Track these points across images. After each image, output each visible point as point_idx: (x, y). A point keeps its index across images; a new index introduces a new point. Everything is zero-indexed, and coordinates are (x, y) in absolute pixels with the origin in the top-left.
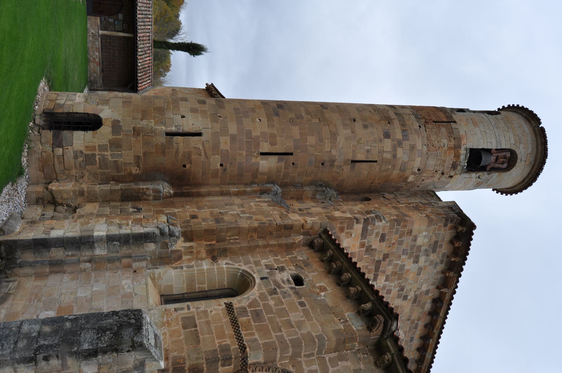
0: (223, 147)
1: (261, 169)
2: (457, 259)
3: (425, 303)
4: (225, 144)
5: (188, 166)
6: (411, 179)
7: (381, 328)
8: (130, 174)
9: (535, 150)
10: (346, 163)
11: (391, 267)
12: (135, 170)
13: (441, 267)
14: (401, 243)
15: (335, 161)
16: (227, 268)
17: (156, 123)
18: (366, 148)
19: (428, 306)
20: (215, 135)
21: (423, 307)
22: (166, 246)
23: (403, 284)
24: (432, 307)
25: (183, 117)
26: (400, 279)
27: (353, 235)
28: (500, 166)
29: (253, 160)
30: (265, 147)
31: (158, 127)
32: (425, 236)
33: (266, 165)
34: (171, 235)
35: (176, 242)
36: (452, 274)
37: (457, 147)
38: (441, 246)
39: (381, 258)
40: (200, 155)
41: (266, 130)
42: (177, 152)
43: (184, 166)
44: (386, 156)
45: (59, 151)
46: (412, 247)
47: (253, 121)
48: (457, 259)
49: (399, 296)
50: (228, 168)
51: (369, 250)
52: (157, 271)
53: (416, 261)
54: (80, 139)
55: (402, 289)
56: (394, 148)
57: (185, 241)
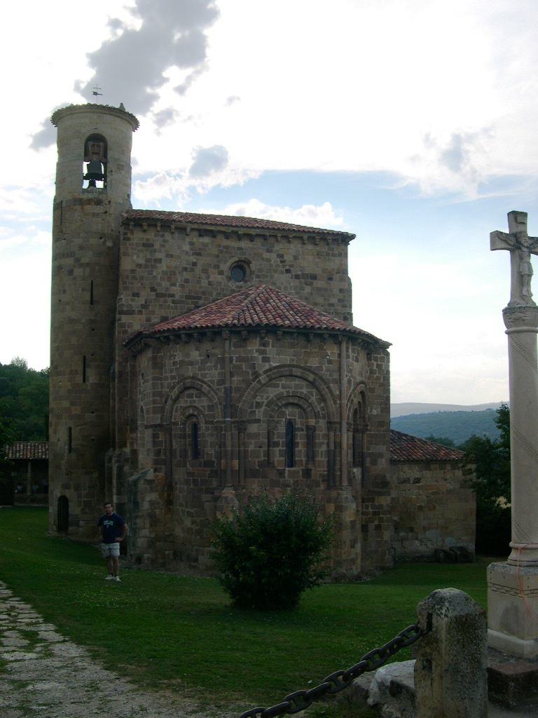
1: (97, 382)
2: (159, 224)
3: (203, 244)
4: (76, 410)
5: (93, 438)
6: (109, 244)
7: (149, 339)
12: (96, 475)
13: (168, 236)
14: (142, 278)
15: (91, 320)
18: (80, 292)
19: (206, 240)
21: (206, 245)
22: (126, 460)
23: (180, 269)
24: (207, 235)
25: (59, 440)
26: (175, 272)
27: (131, 321)
28: (102, 149)
29: (89, 388)
30: (79, 379)
31: (66, 458)
32: (138, 257)
33: (92, 378)
35: (125, 453)
36: (173, 227)
37: (81, 202)
38: (148, 239)
39: (154, 293)
43: (93, 440)
44: (87, 274)
45: (82, 523)
46: (146, 266)
48: (159, 224)
49: (192, 270)
51: (145, 306)
52: (140, 467)
53: (160, 261)
54: (74, 509)
55: (185, 269)
56: (81, 265)
57: (126, 447)
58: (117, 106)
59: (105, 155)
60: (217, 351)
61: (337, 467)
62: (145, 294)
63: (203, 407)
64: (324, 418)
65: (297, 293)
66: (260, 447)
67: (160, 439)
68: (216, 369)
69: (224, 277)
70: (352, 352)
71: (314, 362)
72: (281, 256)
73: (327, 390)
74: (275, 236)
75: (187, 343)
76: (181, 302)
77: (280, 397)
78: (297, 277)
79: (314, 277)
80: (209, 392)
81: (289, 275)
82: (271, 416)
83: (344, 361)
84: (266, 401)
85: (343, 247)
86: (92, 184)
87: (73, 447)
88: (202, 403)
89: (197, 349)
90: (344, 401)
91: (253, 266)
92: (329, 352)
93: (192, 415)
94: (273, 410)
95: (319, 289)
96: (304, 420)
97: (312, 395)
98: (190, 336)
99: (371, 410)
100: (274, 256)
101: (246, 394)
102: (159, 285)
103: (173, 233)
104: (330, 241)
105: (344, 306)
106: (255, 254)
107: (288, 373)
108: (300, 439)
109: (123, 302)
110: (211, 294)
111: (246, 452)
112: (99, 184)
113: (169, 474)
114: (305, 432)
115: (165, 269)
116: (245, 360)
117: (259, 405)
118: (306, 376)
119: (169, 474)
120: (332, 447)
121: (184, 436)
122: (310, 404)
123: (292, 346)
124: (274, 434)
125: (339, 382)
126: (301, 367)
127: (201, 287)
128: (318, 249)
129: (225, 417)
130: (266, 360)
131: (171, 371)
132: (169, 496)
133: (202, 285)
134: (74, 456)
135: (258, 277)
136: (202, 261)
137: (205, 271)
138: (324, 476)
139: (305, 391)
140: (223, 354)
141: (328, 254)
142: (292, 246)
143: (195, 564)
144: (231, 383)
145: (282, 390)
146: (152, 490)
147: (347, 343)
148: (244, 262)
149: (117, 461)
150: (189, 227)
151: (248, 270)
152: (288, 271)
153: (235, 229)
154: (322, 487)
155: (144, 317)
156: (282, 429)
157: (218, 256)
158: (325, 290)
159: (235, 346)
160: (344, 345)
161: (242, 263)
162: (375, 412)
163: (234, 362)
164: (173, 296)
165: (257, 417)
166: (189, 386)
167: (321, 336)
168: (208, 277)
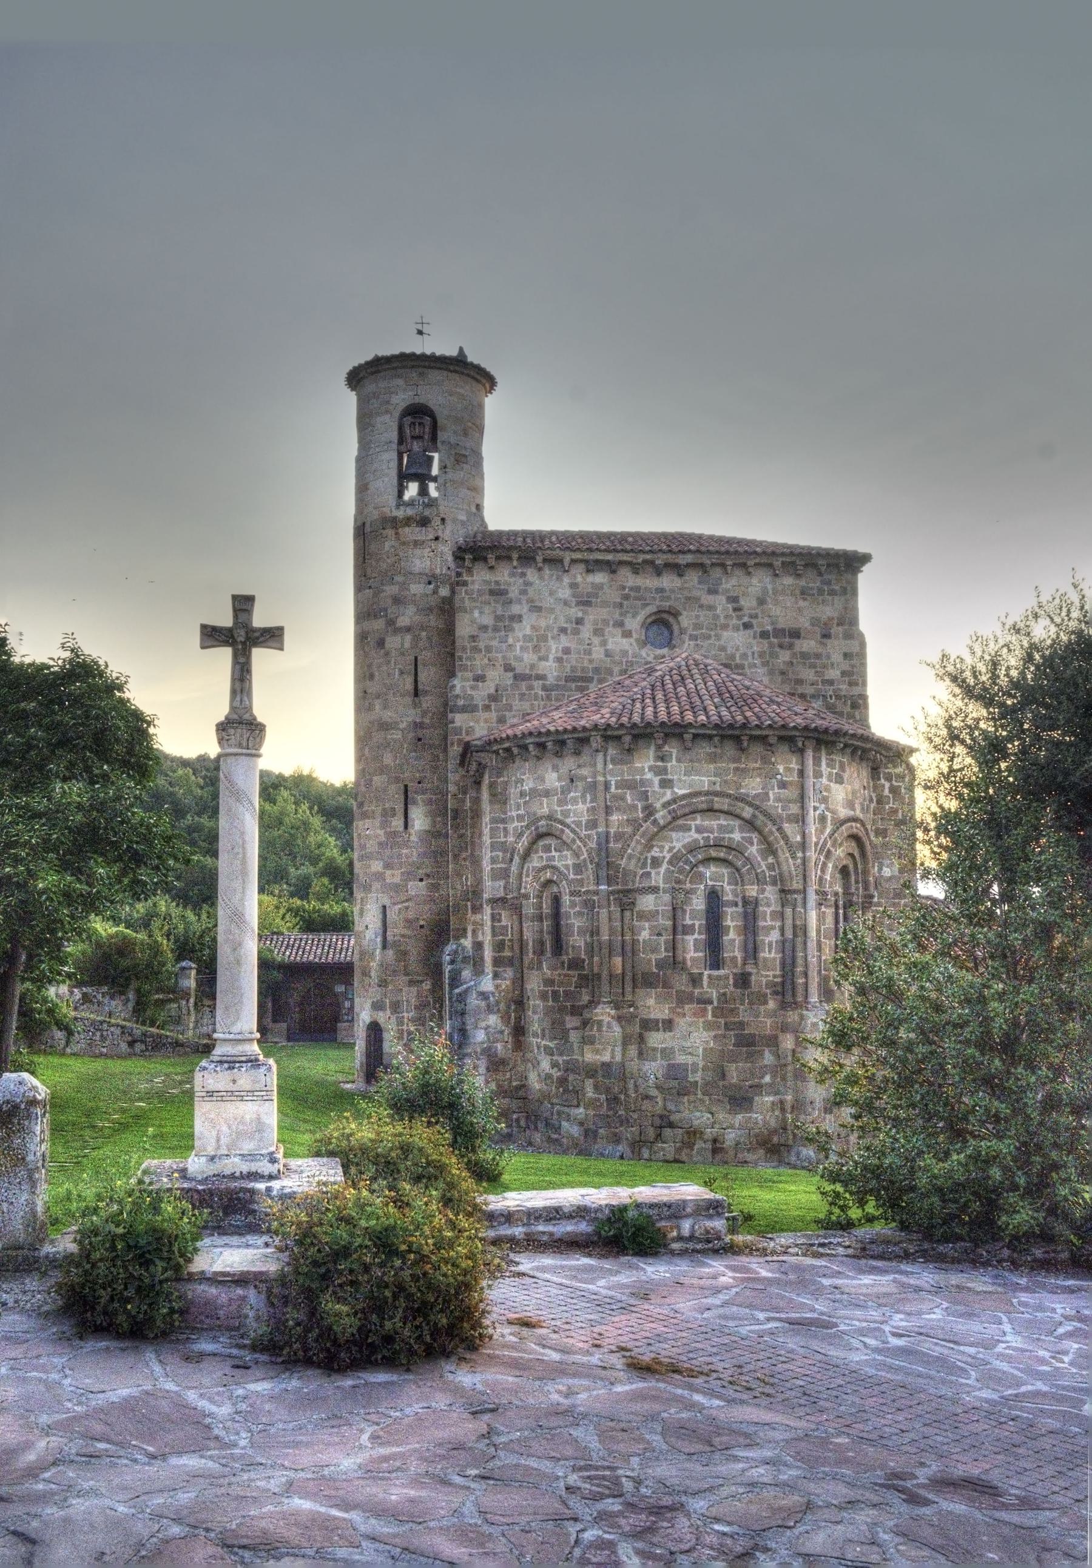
0: (397, 880)
1: (427, 828)
2: (515, 556)
4: (394, 877)
5: (422, 923)
6: (444, 592)
8: (433, 991)
9: (400, 371)
10: (415, 705)
11: (525, 656)
12: (427, 986)
13: (531, 574)
14: (489, 649)
19: (600, 578)
21: (600, 587)
22: (465, 960)
23: (555, 631)
24: (601, 570)
29: (414, 838)
30: (397, 823)
33: (420, 820)
34: (456, 952)
35: (464, 948)
36: (539, 559)
37: (395, 523)
38: (497, 583)
39: (510, 674)
40: (407, 908)
41: (377, 822)
43: (422, 927)
44: (407, 645)
46: (496, 629)
47: (368, 837)
48: (515, 556)
49: (576, 632)
50: (428, 871)
51: (494, 698)
54: (392, 1045)
55: (563, 630)
56: (397, 631)
58: (453, 352)
59: (434, 438)
60: (585, 772)
61: (799, 969)
62: (495, 676)
63: (567, 867)
64: (774, 883)
65: (764, 664)
66: (659, 934)
67: (503, 923)
68: (584, 802)
69: (632, 640)
70: (828, 765)
71: (753, 786)
72: (734, 600)
73: (777, 834)
74: (723, 566)
75: (538, 758)
76: (557, 687)
77: (692, 849)
78: (764, 635)
79: (795, 634)
80: (574, 841)
81: (750, 632)
82: (678, 882)
83: (810, 781)
84: (668, 856)
85: (849, 576)
86: (423, 491)
87: (390, 938)
88: (565, 861)
89: (555, 768)
90: (812, 854)
91: (685, 620)
92: (781, 768)
93: (550, 882)
94: (681, 871)
95: (804, 656)
96: (739, 888)
97: (752, 844)
98: (542, 746)
99: (880, 869)
100: (720, 602)
101: (633, 844)
102: (520, 659)
103: (540, 569)
104: (823, 569)
105: (851, 684)
106: (688, 599)
107: (704, 806)
108: (731, 921)
109: (458, 691)
110: (610, 672)
111: (634, 942)
112: (432, 488)
113: (520, 981)
114: (740, 909)
115: (528, 631)
116: (631, 785)
117: (656, 862)
118: (738, 811)
119: (520, 981)
120: (789, 934)
121: (540, 918)
122: (747, 859)
123: (713, 758)
124: (684, 911)
125: (801, 819)
126: (729, 796)
127: (591, 661)
128: (802, 583)
129: (598, 884)
130: (666, 784)
131: (518, 808)
132: (518, 1019)
133: (594, 656)
134: (390, 953)
135: (693, 638)
136: (593, 616)
137: (598, 632)
138: (775, 985)
139: (737, 836)
140: (594, 776)
141: (821, 592)
142: (754, 581)
143: (555, 1136)
144: (607, 826)
145: (696, 836)
146: (490, 1009)
147: (817, 750)
148: (669, 612)
149: (452, 962)
150: (567, 557)
151: (676, 628)
152: (747, 626)
153: (648, 557)
154: (771, 1005)
155: (494, 715)
156: (698, 903)
157: (621, 605)
158: (818, 656)
159: (613, 761)
160: (809, 754)
161: (665, 616)
162: (887, 872)
163: (613, 789)
164: (542, 677)
165: (653, 883)
166: (543, 834)
167: (763, 739)
168: (604, 643)
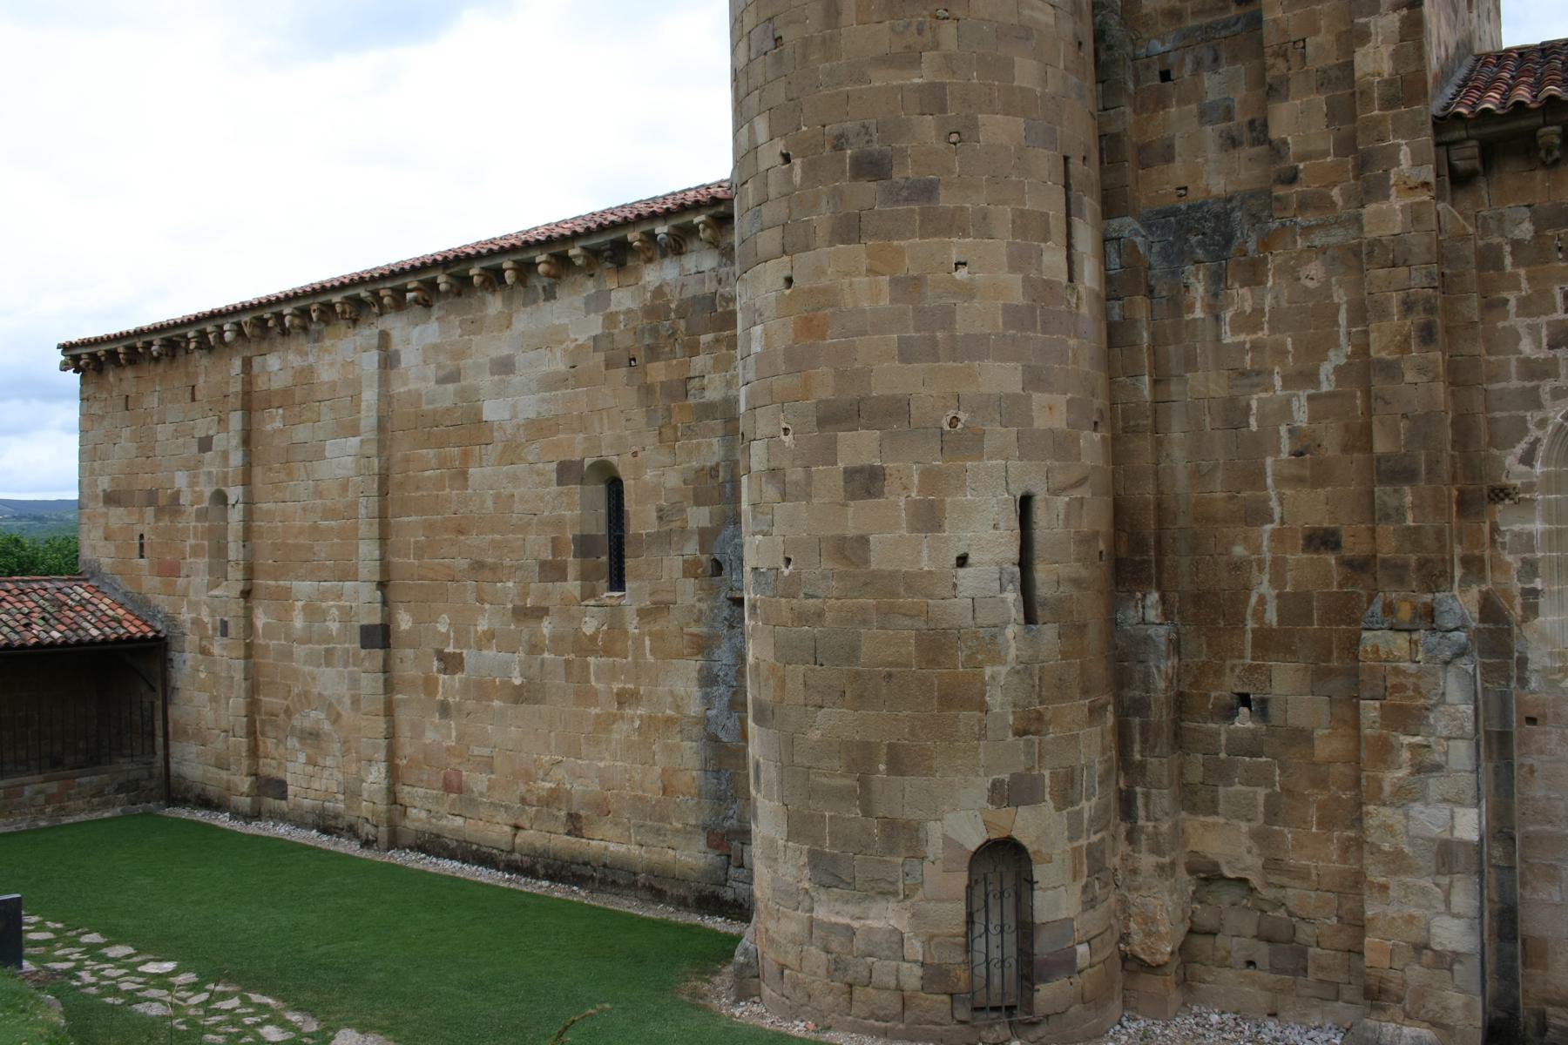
0: (1059, 421)
16: (1546, 463)
17: (997, 658)
20: (1030, 444)
30: (1053, 259)
31: (1013, 652)
41: (1000, 246)
42: (1077, 582)
47: (968, 292)
54: (1057, 899)
134: (1048, 632)
